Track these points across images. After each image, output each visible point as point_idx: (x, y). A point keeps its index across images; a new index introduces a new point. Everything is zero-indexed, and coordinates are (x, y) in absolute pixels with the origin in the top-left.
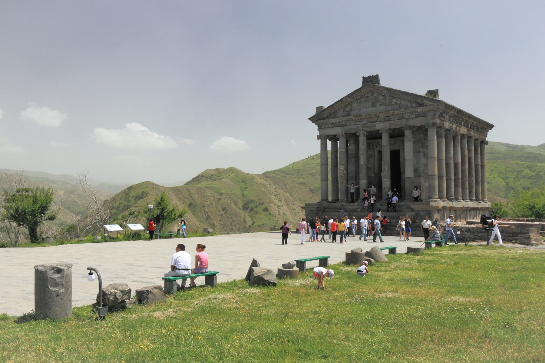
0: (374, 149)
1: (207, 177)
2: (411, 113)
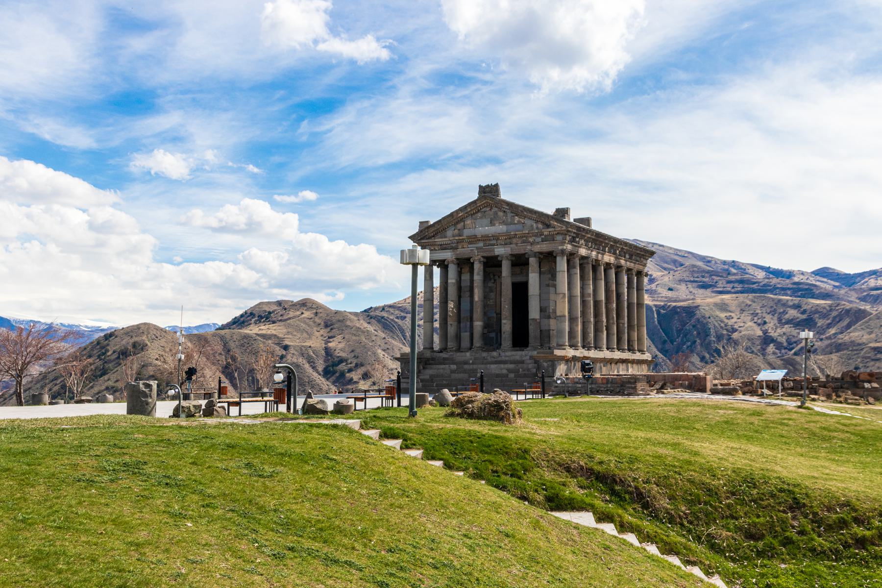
1: (261, 317)
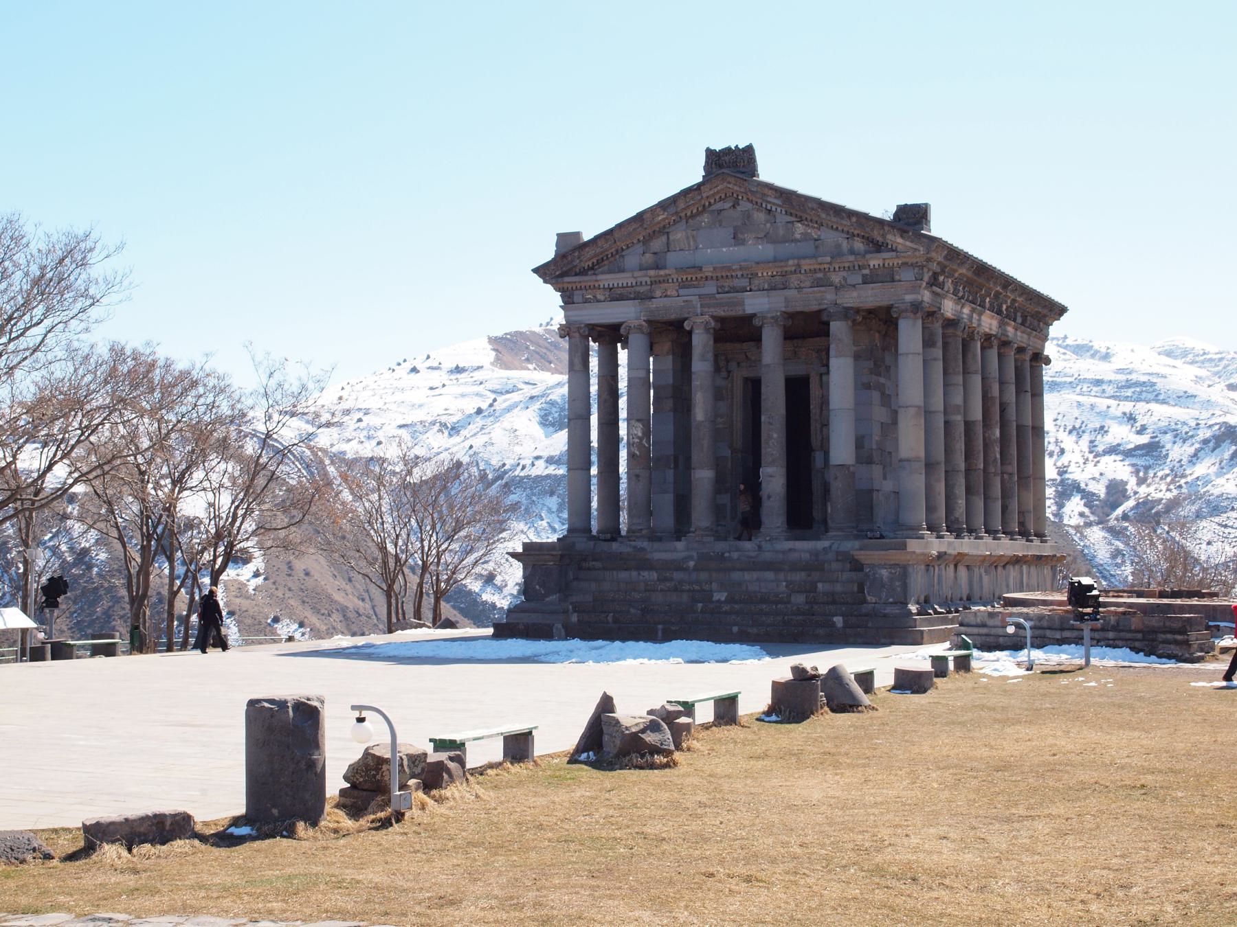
0: (729, 372)
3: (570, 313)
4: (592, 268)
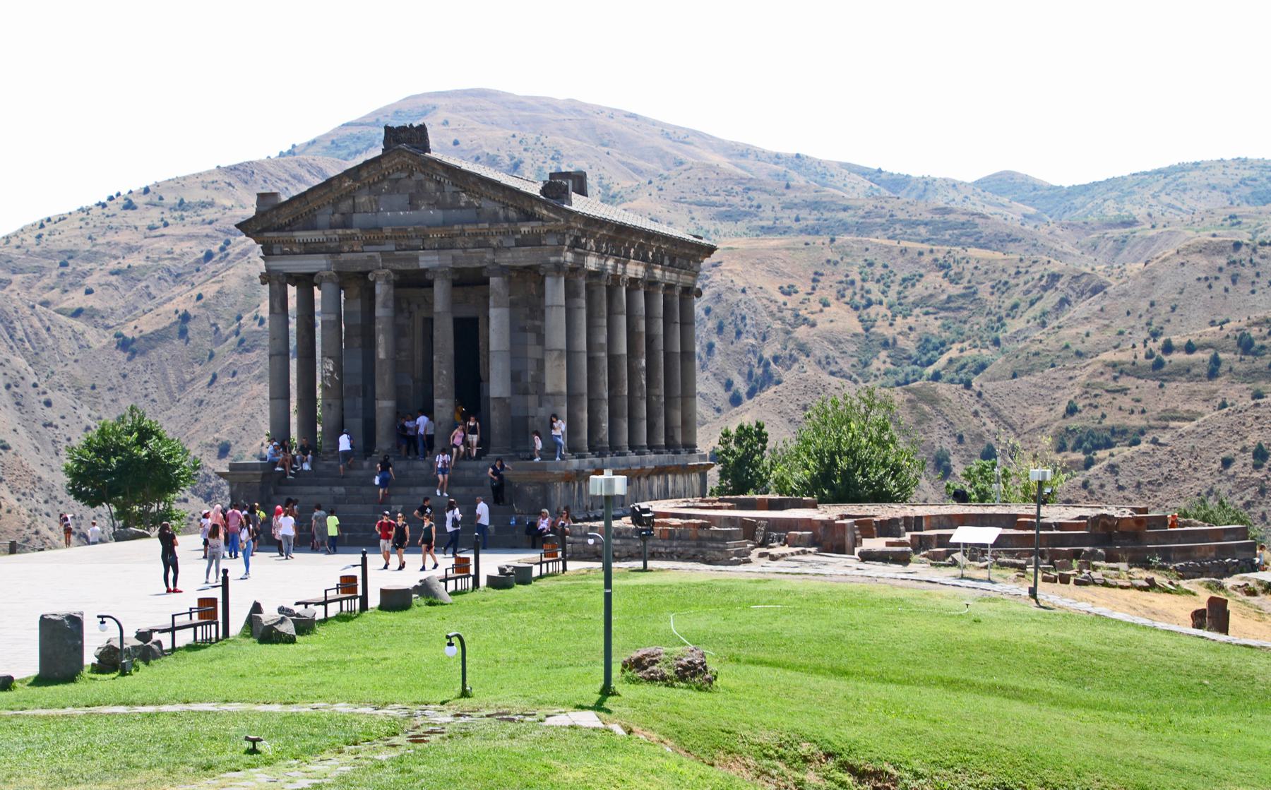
2: (505, 234)
3: (270, 263)
4: (289, 227)
